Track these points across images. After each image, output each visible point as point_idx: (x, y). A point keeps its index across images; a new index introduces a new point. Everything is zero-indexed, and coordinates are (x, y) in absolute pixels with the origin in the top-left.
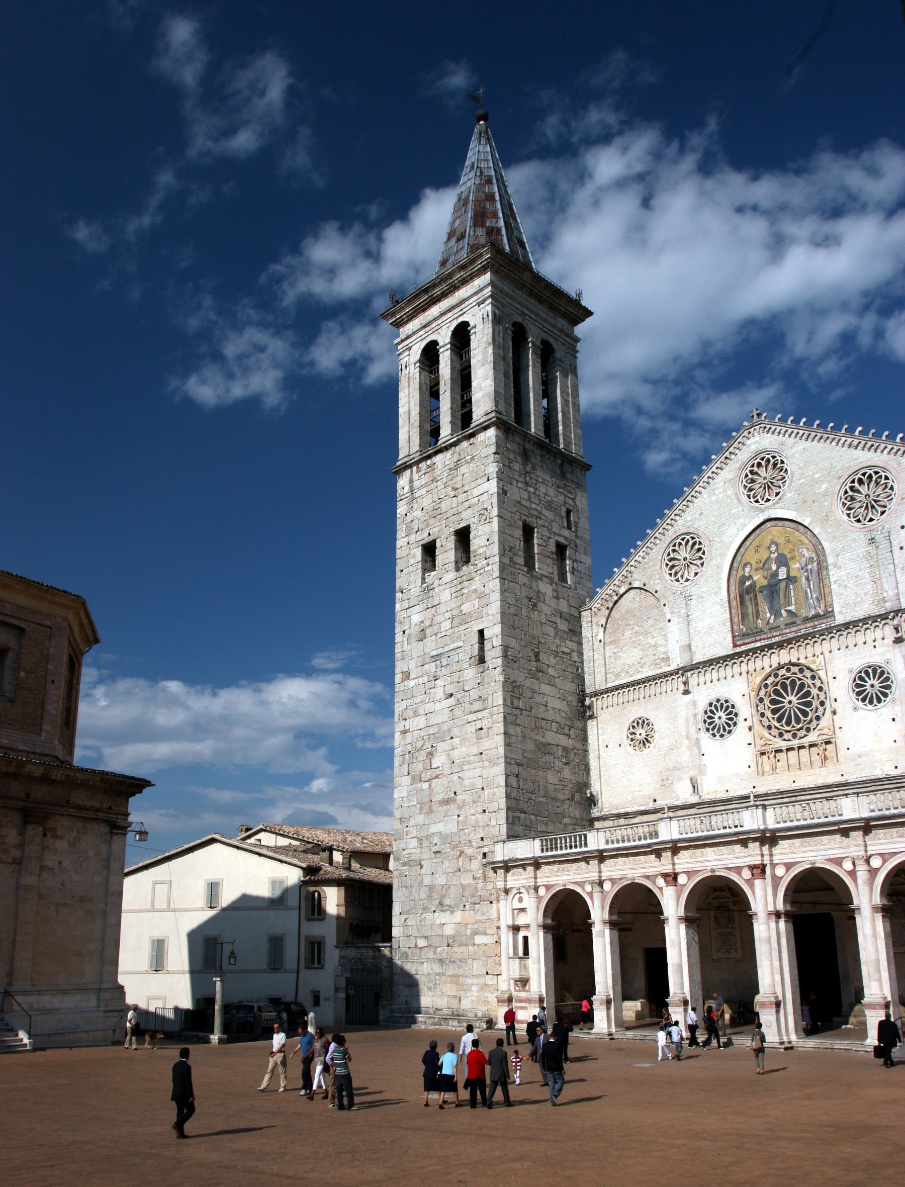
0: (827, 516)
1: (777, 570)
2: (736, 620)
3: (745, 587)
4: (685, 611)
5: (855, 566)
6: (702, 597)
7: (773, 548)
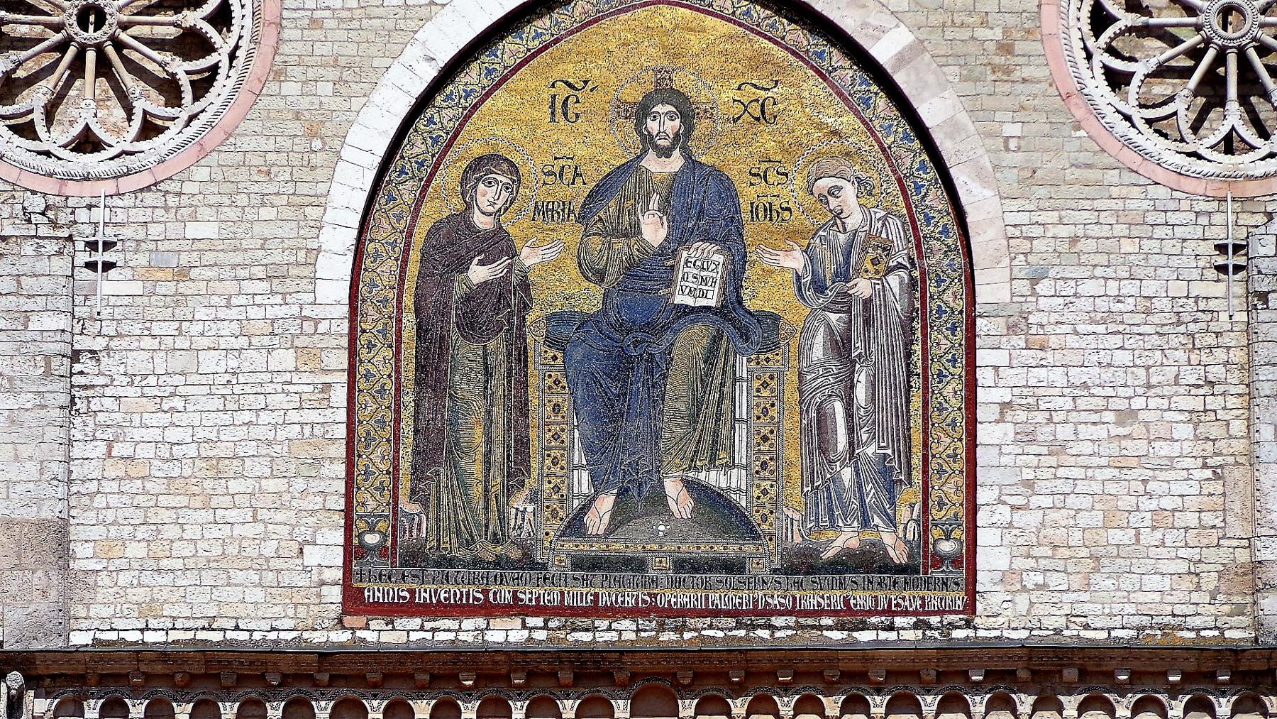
0: (1006, 48)
1: (668, 251)
2: (377, 458)
3: (459, 290)
4: (63, 322)
5: (1123, 358)
6: (182, 274)
7: (664, 124)
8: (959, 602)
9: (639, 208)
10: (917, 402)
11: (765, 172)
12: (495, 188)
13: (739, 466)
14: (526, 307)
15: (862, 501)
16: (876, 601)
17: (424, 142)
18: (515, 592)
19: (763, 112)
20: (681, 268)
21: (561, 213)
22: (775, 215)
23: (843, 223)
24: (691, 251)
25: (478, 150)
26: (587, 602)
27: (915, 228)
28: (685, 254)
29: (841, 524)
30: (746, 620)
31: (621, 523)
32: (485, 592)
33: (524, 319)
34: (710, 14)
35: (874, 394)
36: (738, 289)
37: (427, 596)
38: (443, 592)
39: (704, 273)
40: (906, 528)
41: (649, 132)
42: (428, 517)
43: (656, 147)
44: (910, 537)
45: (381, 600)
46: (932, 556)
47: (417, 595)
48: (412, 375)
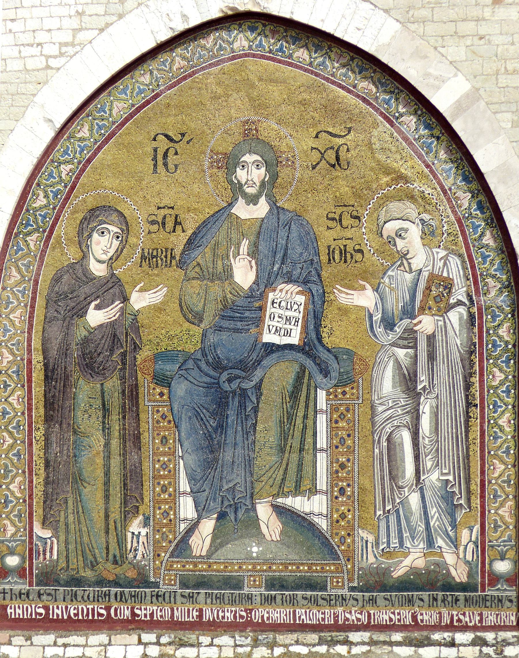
8: (513, 618)
9: (231, 254)
10: (475, 433)
11: (341, 216)
12: (107, 237)
13: (321, 492)
14: (136, 348)
15: (427, 524)
16: (440, 617)
17: (46, 196)
18: (133, 608)
19: (338, 158)
20: (268, 309)
21: (164, 259)
22: (348, 256)
23: (409, 264)
24: (277, 292)
25: (91, 203)
26: (193, 618)
27: (473, 267)
28: (271, 296)
29: (409, 545)
30: (326, 635)
31: (221, 545)
32: (108, 609)
33: (135, 358)
34: (290, 64)
35: (437, 424)
36: (318, 327)
37: (60, 612)
38: (73, 608)
39: (289, 313)
40: (466, 548)
41: (238, 181)
42: (58, 541)
43: (245, 195)
44: (469, 557)
45: (21, 617)
46: (489, 576)
47: (51, 612)
48: (42, 411)
